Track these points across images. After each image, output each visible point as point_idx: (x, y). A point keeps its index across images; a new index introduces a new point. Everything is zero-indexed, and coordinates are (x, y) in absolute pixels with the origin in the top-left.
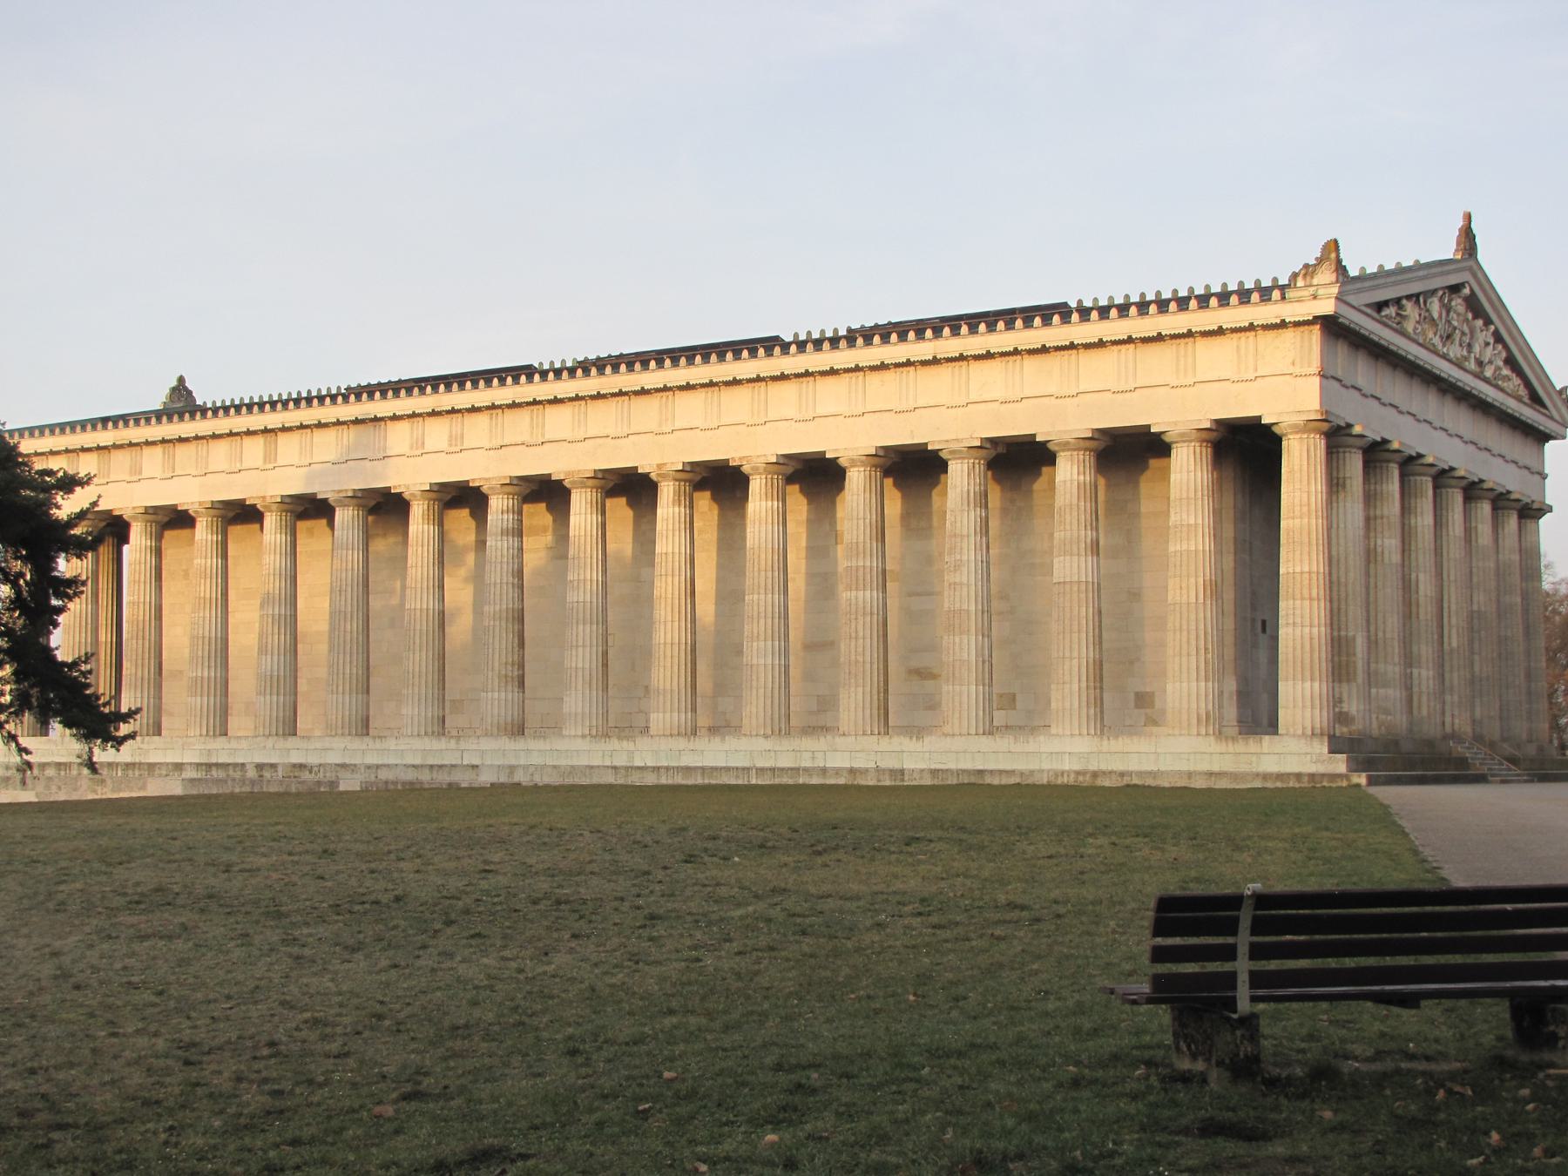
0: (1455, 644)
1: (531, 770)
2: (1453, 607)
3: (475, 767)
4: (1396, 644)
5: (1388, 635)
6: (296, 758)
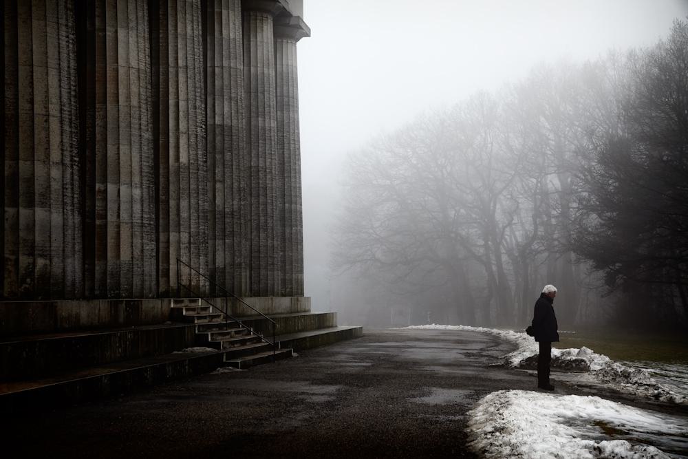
0: (183, 159)
2: (182, 104)
4: (54, 125)
5: (38, 108)
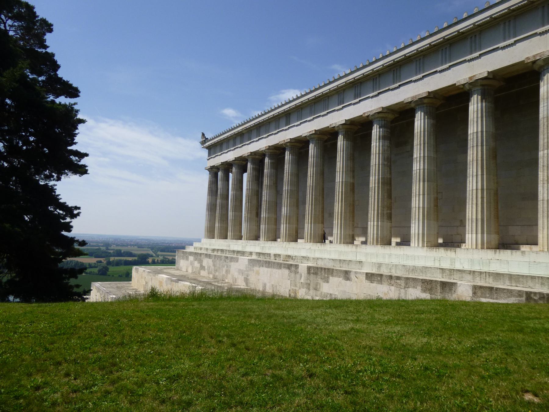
1: (390, 267)
3: (360, 262)
6: (289, 253)
